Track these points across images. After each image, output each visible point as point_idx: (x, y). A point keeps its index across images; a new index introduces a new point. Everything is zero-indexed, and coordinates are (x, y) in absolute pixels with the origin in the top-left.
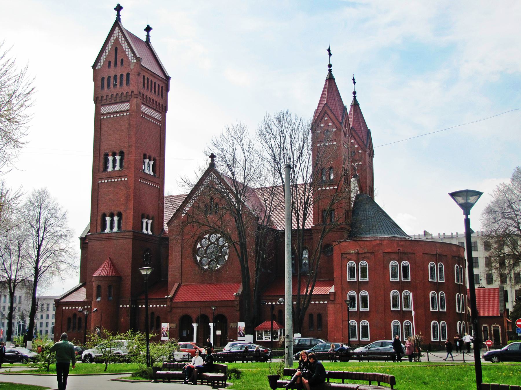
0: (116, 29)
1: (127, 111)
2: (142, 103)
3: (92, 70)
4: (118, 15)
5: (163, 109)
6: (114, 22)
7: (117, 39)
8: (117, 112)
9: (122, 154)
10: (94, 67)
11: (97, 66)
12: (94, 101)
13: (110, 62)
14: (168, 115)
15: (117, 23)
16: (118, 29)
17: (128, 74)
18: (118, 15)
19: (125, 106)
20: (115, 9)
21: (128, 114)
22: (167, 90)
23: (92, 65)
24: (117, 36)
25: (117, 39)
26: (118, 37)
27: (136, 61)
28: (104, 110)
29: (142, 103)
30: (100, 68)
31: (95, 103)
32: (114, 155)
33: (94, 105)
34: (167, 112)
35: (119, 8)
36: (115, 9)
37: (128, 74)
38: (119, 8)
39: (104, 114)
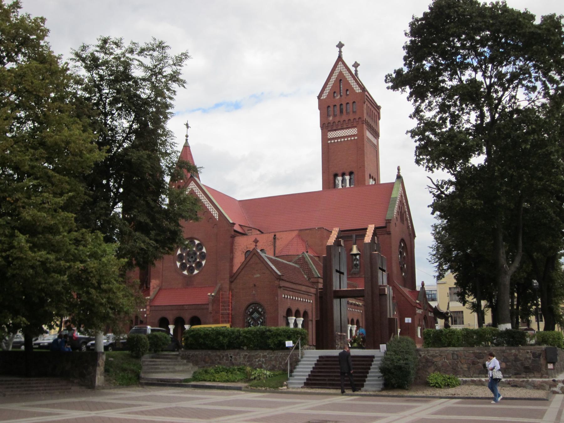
1: (354, 136)
3: (317, 101)
4: (340, 52)
5: (376, 134)
6: (337, 57)
7: (341, 73)
8: (344, 137)
9: (351, 174)
10: (319, 97)
11: (322, 96)
12: (321, 127)
13: (335, 92)
14: (380, 140)
15: (340, 58)
18: (340, 52)
19: (354, 131)
20: (337, 46)
21: (356, 138)
22: (379, 119)
23: (318, 95)
25: (341, 73)
28: (331, 135)
31: (321, 129)
32: (343, 175)
33: (320, 130)
34: (380, 138)
35: (340, 45)
36: (337, 46)
37: (354, 102)
38: (340, 45)
39: (331, 139)
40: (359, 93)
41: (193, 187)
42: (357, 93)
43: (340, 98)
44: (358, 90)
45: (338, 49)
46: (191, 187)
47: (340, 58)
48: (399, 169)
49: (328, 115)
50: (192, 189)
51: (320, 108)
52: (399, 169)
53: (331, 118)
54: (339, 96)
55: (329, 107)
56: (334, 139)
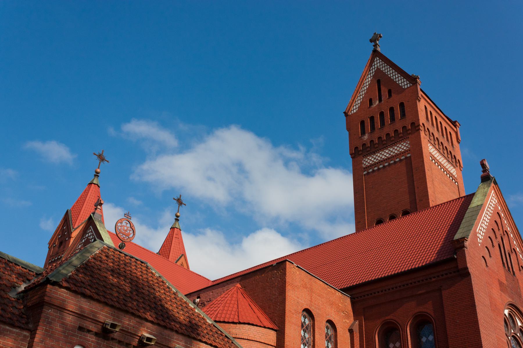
0: (375, 60)
2: (429, 141)
4: (375, 45)
7: (378, 70)
15: (376, 53)
16: (378, 58)
17: (402, 105)
19: (402, 147)
20: (371, 41)
24: (377, 67)
25: (378, 70)
26: (379, 67)
27: (411, 85)
29: (429, 141)
30: (355, 111)
36: (371, 41)
40: (408, 88)
41: (90, 234)
42: (405, 89)
43: (378, 105)
44: (404, 83)
45: (373, 44)
46: (87, 235)
47: (376, 53)
48: (483, 165)
49: (363, 133)
50: (88, 236)
51: (348, 129)
52: (483, 165)
53: (366, 137)
54: (377, 102)
55: (362, 123)
56: (371, 166)
